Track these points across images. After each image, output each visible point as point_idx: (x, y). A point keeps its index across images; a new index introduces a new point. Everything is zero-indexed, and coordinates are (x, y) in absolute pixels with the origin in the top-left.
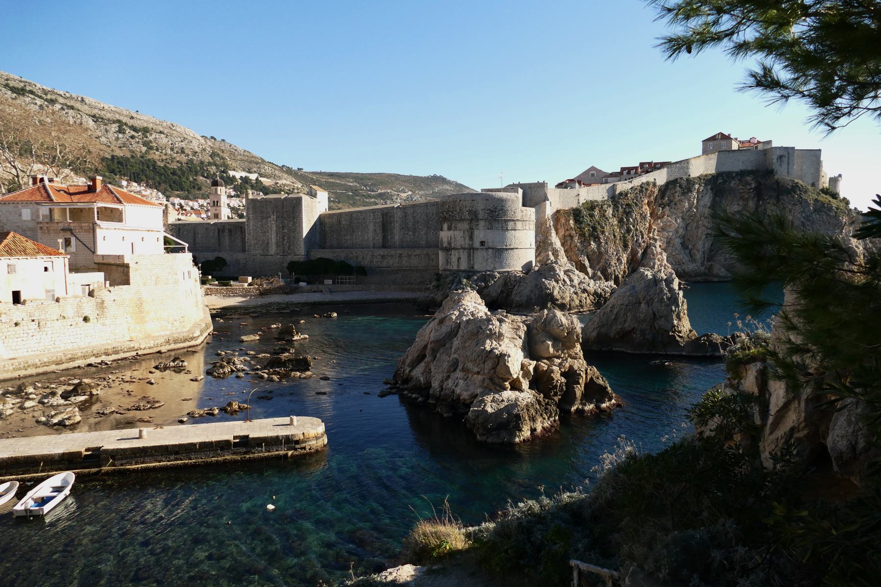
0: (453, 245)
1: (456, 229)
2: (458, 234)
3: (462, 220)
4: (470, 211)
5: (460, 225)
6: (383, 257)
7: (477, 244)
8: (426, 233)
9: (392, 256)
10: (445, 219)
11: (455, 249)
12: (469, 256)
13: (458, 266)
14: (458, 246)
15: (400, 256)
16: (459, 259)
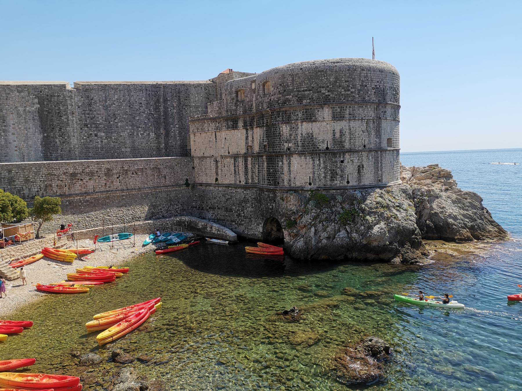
0: (347, 145)
1: (353, 117)
2: (358, 126)
3: (364, 102)
4: (376, 88)
5: (360, 112)
6: (73, 175)
7: (384, 144)
8: (131, 135)
9: (91, 174)
10: (326, 101)
11: (351, 151)
12: (376, 162)
13: (359, 179)
14: (358, 144)
15: (108, 173)
16: (360, 168)
